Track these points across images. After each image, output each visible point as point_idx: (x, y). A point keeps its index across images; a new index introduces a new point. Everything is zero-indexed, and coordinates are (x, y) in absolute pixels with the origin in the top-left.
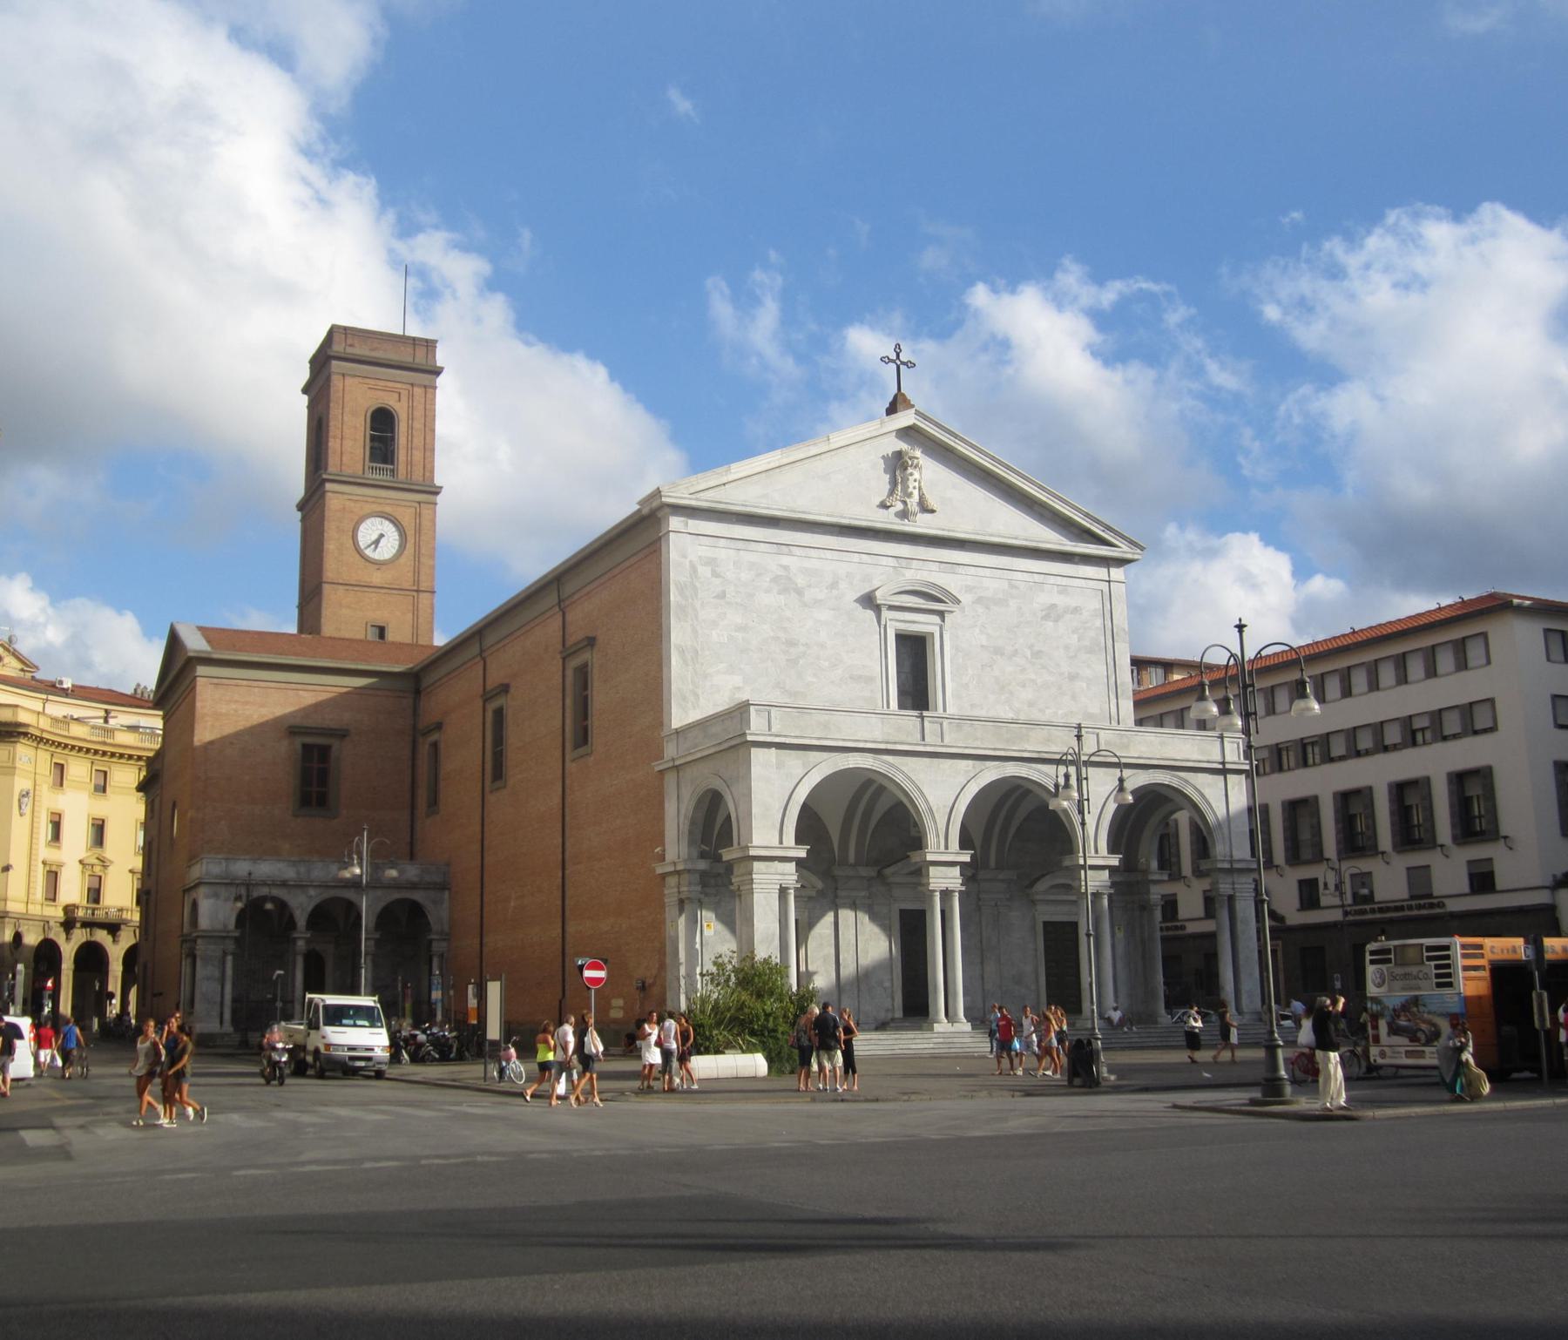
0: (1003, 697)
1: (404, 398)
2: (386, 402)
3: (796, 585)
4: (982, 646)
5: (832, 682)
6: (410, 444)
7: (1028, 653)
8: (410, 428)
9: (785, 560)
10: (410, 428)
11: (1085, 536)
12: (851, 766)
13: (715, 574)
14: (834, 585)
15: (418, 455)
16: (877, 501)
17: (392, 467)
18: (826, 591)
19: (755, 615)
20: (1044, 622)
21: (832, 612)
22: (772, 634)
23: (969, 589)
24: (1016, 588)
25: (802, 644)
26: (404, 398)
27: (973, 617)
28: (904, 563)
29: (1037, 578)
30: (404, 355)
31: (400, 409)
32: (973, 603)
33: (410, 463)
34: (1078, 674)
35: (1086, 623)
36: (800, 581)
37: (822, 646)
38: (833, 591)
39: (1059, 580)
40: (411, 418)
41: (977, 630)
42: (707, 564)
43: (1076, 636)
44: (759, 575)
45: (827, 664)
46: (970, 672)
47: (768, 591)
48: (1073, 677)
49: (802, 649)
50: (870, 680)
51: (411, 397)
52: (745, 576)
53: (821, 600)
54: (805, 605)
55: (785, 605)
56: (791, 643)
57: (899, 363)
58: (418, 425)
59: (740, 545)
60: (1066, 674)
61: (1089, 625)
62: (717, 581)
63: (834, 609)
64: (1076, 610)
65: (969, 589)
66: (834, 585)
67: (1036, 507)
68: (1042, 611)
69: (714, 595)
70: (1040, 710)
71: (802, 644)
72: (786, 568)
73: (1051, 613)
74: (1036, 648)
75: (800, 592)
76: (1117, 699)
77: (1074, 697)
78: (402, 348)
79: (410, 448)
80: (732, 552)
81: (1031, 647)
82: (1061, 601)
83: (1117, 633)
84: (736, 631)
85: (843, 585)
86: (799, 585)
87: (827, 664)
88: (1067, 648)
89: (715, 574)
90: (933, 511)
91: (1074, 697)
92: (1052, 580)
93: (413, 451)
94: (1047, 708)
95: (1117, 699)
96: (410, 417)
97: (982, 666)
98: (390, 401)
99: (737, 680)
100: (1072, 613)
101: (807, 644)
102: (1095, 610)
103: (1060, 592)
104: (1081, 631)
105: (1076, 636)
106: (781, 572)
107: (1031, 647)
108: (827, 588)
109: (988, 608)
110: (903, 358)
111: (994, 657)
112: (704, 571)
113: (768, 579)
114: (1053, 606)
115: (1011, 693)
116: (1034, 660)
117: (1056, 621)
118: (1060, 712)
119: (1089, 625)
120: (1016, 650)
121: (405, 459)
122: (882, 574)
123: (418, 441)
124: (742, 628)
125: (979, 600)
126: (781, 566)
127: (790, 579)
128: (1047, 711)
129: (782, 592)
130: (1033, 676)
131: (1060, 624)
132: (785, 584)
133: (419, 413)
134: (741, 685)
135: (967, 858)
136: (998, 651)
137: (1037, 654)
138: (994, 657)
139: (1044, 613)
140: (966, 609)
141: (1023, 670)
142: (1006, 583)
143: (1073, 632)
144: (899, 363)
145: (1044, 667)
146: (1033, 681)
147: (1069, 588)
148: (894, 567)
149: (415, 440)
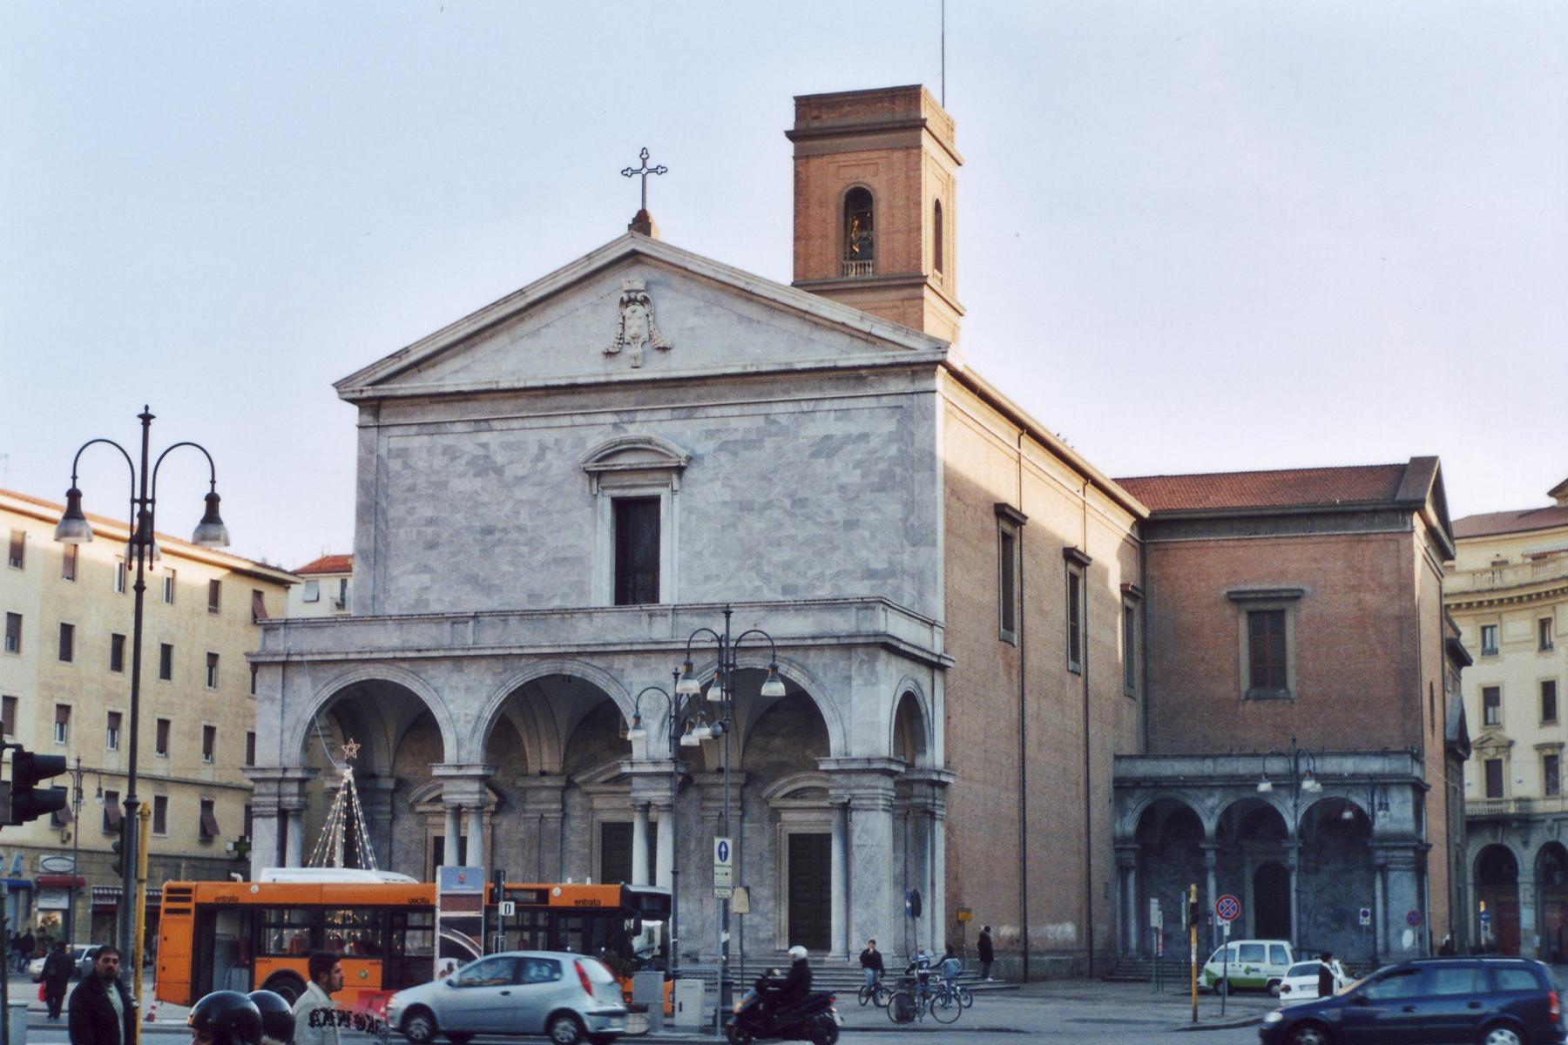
0: (749, 562)
2: (860, 180)
3: (496, 463)
4: (725, 503)
7: (787, 504)
9: (485, 437)
12: (363, 679)
13: (406, 466)
16: (603, 347)
21: (537, 489)
22: (464, 523)
23: (710, 434)
24: (775, 422)
25: (499, 530)
27: (715, 468)
28: (625, 417)
29: (805, 406)
31: (878, 184)
32: (715, 451)
35: (874, 453)
36: (500, 459)
39: (837, 404)
41: (719, 483)
42: (398, 456)
43: (858, 472)
44: (453, 459)
47: (463, 475)
48: (851, 525)
55: (483, 488)
56: (488, 531)
57: (644, 171)
59: (432, 429)
60: (841, 522)
61: (878, 454)
62: (409, 472)
64: (864, 437)
65: (710, 434)
68: (811, 446)
70: (799, 573)
71: (499, 530)
72: (485, 446)
73: (826, 448)
74: (799, 496)
77: (850, 552)
80: (425, 439)
81: (791, 496)
82: (837, 428)
84: (426, 525)
85: (550, 456)
86: (499, 464)
92: (827, 405)
94: (811, 568)
97: (723, 527)
99: (426, 578)
100: (853, 443)
105: (858, 472)
106: (481, 452)
107: (791, 496)
108: (531, 462)
109: (735, 454)
110: (637, 165)
111: (740, 514)
112: (395, 465)
113: (464, 462)
114: (828, 437)
115: (761, 556)
118: (828, 572)
119: (878, 454)
120: (771, 501)
124: (431, 522)
125: (723, 447)
127: (487, 457)
128: (811, 573)
130: (792, 531)
131: (836, 458)
132: (484, 466)
134: (429, 584)
136: (746, 507)
137: (799, 502)
139: (814, 449)
140: (706, 459)
141: (781, 525)
142: (763, 417)
143: (854, 468)
144: (644, 171)
146: (793, 538)
147: (853, 411)
148: (615, 425)
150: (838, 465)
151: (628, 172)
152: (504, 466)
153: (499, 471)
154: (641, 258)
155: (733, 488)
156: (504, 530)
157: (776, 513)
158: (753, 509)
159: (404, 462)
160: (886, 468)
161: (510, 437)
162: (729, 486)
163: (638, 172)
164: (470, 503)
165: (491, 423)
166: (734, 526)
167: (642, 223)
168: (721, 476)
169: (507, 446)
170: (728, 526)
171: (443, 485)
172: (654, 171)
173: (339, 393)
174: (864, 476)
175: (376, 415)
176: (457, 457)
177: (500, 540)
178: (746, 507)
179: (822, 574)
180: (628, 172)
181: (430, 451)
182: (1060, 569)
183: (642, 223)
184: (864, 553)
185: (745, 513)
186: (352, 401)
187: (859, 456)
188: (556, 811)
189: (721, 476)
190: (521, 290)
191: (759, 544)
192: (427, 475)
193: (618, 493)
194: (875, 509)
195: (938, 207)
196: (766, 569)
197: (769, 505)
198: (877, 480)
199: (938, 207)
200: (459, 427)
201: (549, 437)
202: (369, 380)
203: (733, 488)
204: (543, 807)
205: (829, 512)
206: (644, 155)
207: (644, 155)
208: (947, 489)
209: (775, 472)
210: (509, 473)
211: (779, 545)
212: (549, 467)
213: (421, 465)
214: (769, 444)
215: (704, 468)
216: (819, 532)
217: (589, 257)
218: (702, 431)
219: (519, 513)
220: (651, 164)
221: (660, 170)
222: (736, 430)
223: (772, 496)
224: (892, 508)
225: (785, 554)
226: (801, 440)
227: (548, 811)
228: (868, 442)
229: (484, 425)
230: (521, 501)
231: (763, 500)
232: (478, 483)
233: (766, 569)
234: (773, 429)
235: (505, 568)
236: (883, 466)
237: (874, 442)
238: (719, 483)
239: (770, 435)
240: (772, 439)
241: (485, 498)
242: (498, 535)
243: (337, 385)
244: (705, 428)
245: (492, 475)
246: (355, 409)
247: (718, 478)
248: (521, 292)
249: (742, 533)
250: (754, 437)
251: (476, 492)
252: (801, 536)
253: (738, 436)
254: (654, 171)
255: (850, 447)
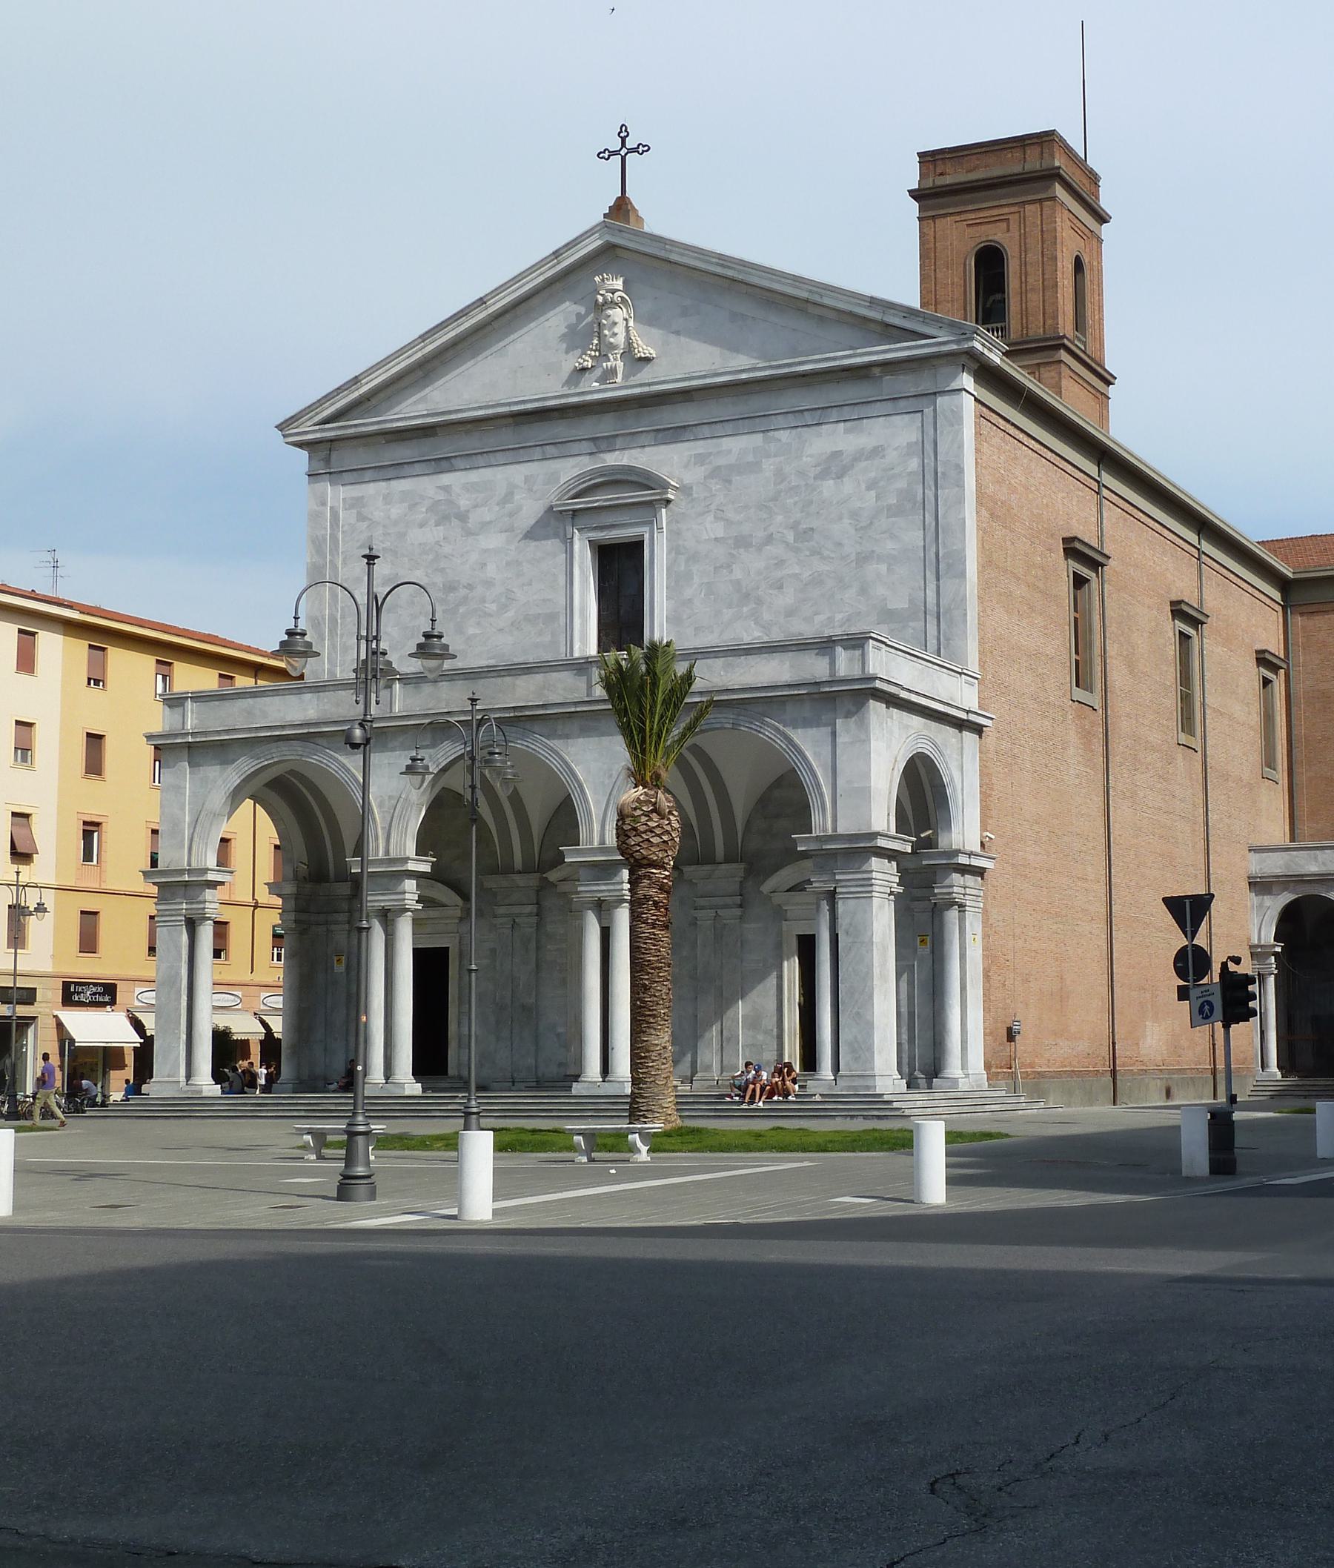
0: (745, 609)
1: (1014, 225)
3: (459, 508)
4: (716, 539)
5: (500, 630)
6: (1024, 285)
7: (790, 537)
8: (1023, 264)
9: (446, 479)
10: (1023, 264)
11: (895, 332)
13: (361, 518)
14: (508, 497)
15: (1035, 299)
17: (1003, 324)
18: (497, 508)
19: (406, 559)
20: (819, 482)
21: (504, 535)
25: (464, 587)
26: (1014, 225)
27: (705, 498)
30: (1010, 165)
33: (1025, 313)
34: (873, 551)
36: (464, 503)
37: (489, 584)
38: (506, 506)
40: (1024, 249)
41: (710, 518)
42: (352, 506)
43: (873, 493)
44: (413, 506)
45: (494, 607)
46: (696, 579)
47: (421, 526)
48: (863, 559)
49: (463, 592)
50: (552, 617)
51: (1022, 220)
52: (396, 511)
53: (490, 522)
54: (469, 533)
57: (623, 152)
58: (1034, 256)
59: (391, 473)
60: (853, 557)
63: (506, 532)
64: (877, 452)
65: (701, 459)
66: (508, 497)
67: (811, 309)
69: (359, 544)
71: (464, 587)
72: (446, 489)
75: (463, 517)
76: (938, 580)
77: (863, 591)
78: (1010, 155)
79: (1023, 293)
81: (794, 526)
83: (943, 474)
87: (494, 607)
88: (855, 515)
89: (361, 518)
90: (647, 360)
91: (863, 591)
93: (1029, 295)
94: (817, 614)
95: (938, 580)
96: (1023, 248)
97: (715, 568)
98: (997, 234)
100: (866, 460)
101: (469, 585)
102: (909, 445)
103: (847, 431)
104: (882, 483)
107: (794, 526)
108: (498, 504)
111: (734, 552)
113: (424, 510)
115: (759, 602)
116: (800, 545)
117: (840, 476)
118: (839, 617)
119: (895, 471)
121: (1019, 308)
122: (573, 467)
123: (1034, 279)
125: (715, 473)
126: (439, 487)
128: (818, 619)
129: (443, 520)
130: (797, 570)
133: (1034, 242)
135: (425, 867)
136: (742, 542)
137: (805, 534)
138: (734, 552)
139: (819, 469)
140: (694, 488)
141: (780, 563)
143: (868, 489)
144: (623, 152)
145: (816, 552)
146: (796, 576)
149: (1030, 280)
150: (848, 485)
151: (605, 155)
152: (468, 511)
153: (463, 517)
154: (619, 252)
155: (729, 523)
156: (470, 587)
157: (774, 550)
158: (750, 545)
159: (359, 514)
160: (906, 486)
161: (474, 476)
162: (722, 519)
163: (616, 153)
164: (431, 557)
165: (453, 461)
166: (729, 566)
167: (621, 208)
168: (713, 507)
169: (469, 488)
170: (721, 567)
171: (402, 536)
172: (635, 150)
173: (285, 436)
174: (878, 498)
175: (327, 461)
176: (417, 504)
177: (466, 598)
178: (742, 542)
179: (831, 619)
180: (605, 155)
181: (387, 499)
182: (1170, 628)
183: (621, 208)
184: (880, 591)
185: (742, 550)
186: (300, 445)
187: (873, 474)
188: (529, 915)
189: (713, 507)
190: (481, 299)
191: (758, 588)
192: (384, 526)
193: (595, 535)
194: (893, 537)
195: (1078, 265)
196: (767, 616)
197: (769, 539)
198: (895, 501)
199: (1078, 265)
200: (418, 469)
201: (518, 473)
202: (317, 419)
203: (729, 523)
204: (516, 910)
205: (840, 544)
206: (623, 134)
207: (623, 134)
208: (984, 512)
209: (775, 499)
210: (474, 519)
211: (781, 587)
212: (519, 508)
213: (378, 515)
214: (768, 466)
215: (693, 500)
216: (828, 568)
217: (557, 254)
218: (691, 456)
219: (485, 564)
220: (631, 143)
221: (641, 149)
222: (730, 451)
223: (772, 529)
224: (913, 537)
225: (787, 598)
226: (804, 459)
227: (519, 915)
228: (884, 456)
229: (444, 464)
230: (486, 551)
231: (761, 534)
232: (439, 532)
233: (767, 616)
234: (773, 447)
235: (471, 631)
236: (902, 484)
237: (892, 456)
238: (710, 518)
239: (768, 456)
240: (771, 460)
241: (447, 549)
242: (463, 592)
243: (280, 427)
244: (693, 453)
245: (455, 522)
246: (304, 454)
247: (710, 511)
248: (482, 301)
249: (738, 574)
250: (750, 458)
251: (438, 543)
252: (806, 575)
253: (732, 459)
254: (635, 150)
255: (863, 464)
